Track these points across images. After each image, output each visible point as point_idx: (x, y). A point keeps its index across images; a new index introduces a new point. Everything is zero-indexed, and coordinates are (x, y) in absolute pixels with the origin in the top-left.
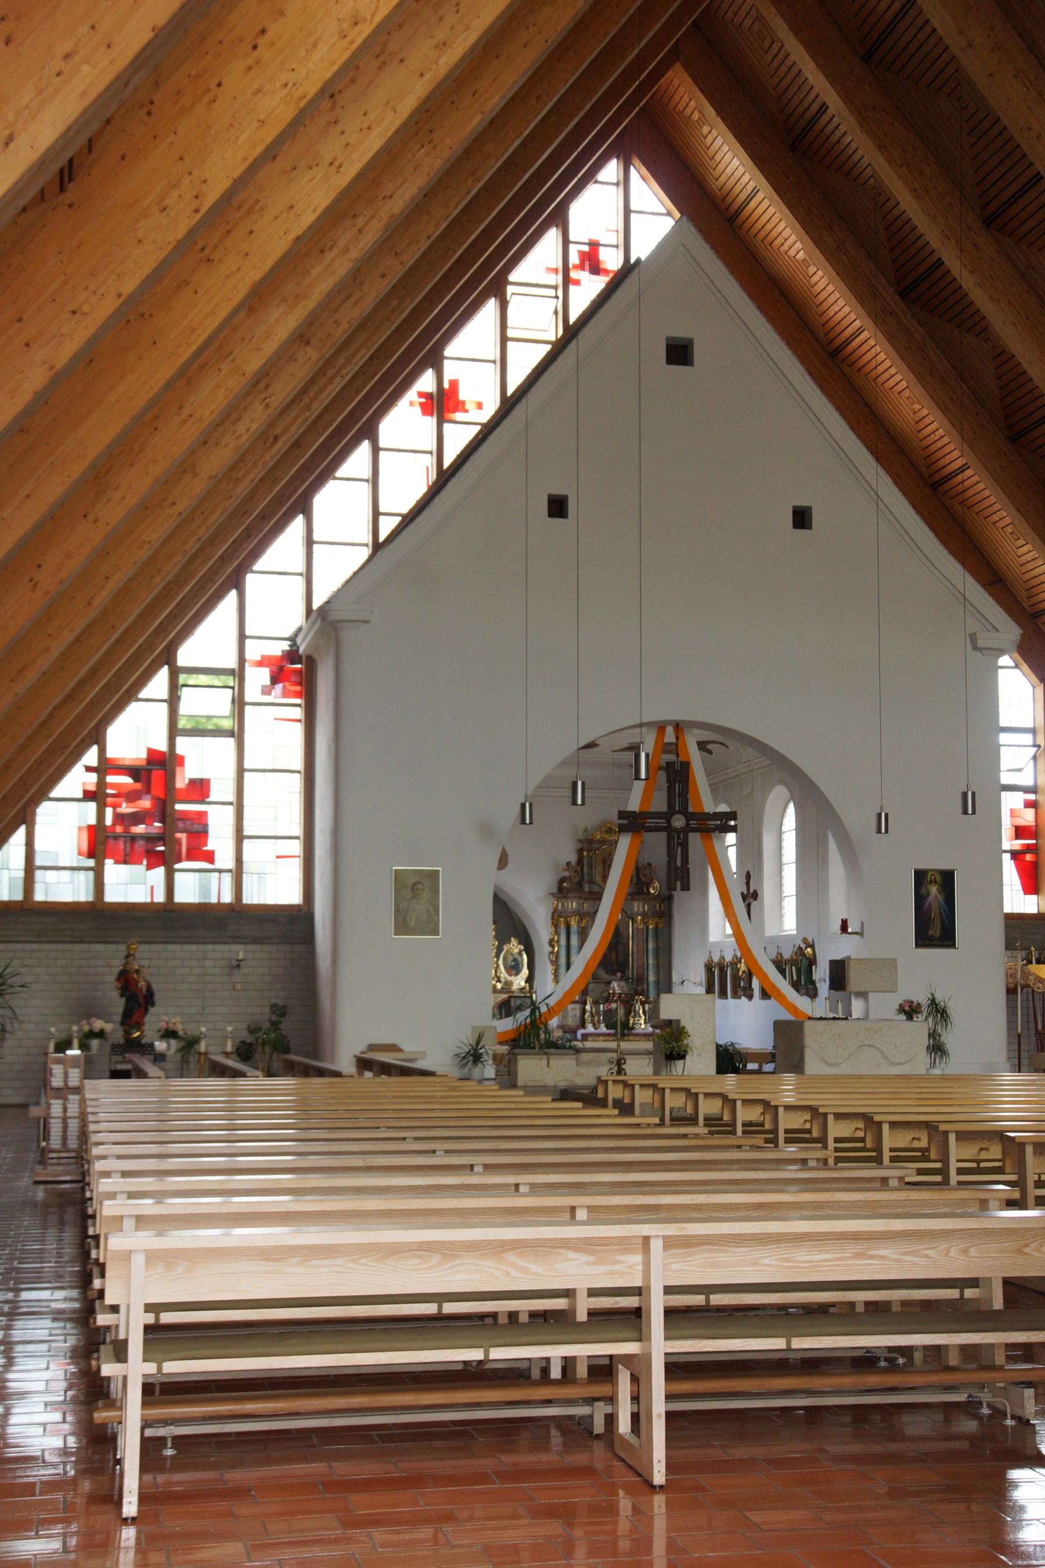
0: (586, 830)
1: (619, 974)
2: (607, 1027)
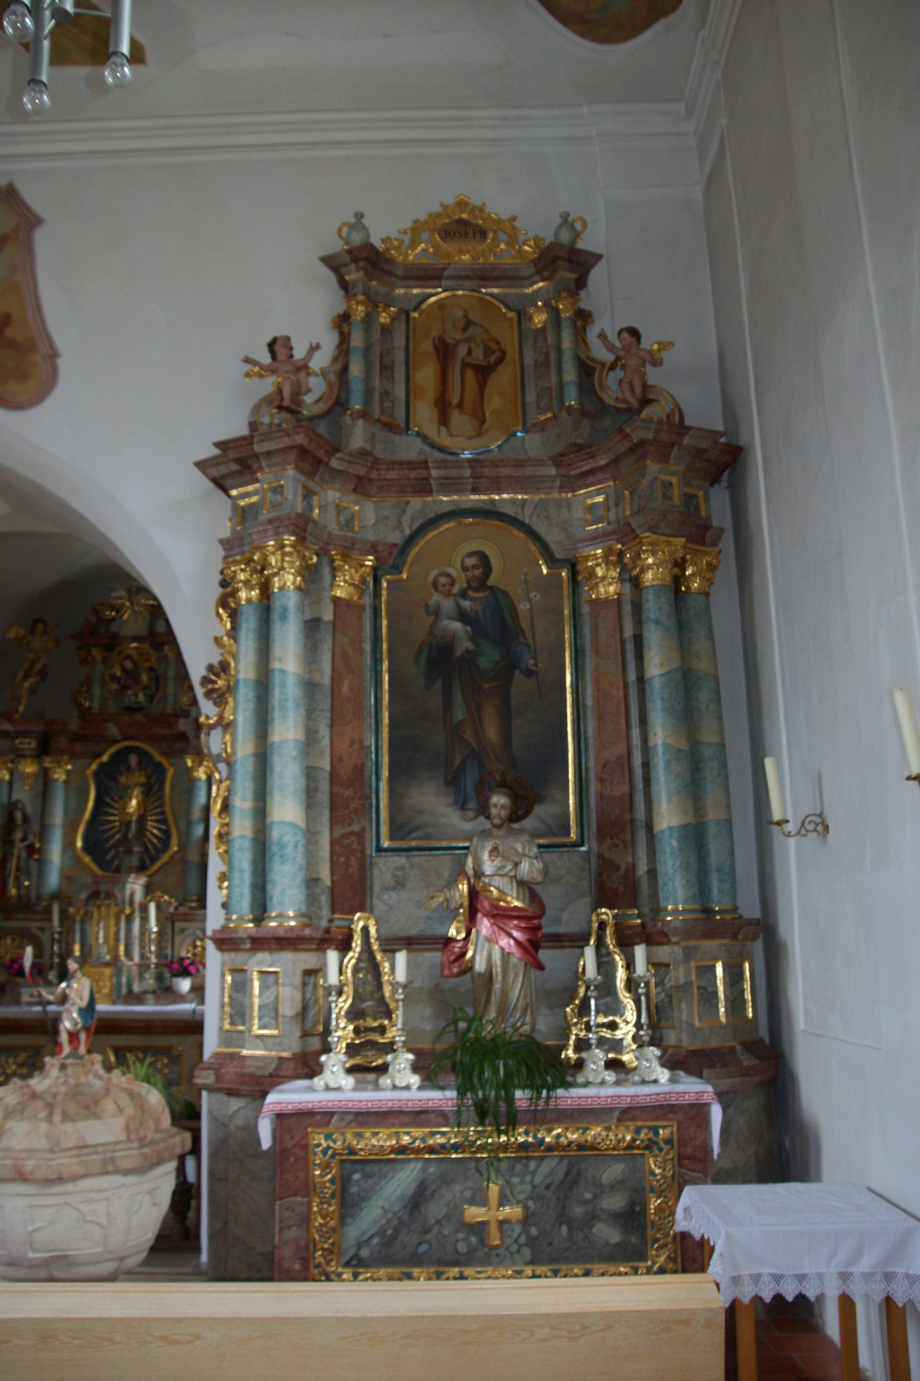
1: (499, 801)
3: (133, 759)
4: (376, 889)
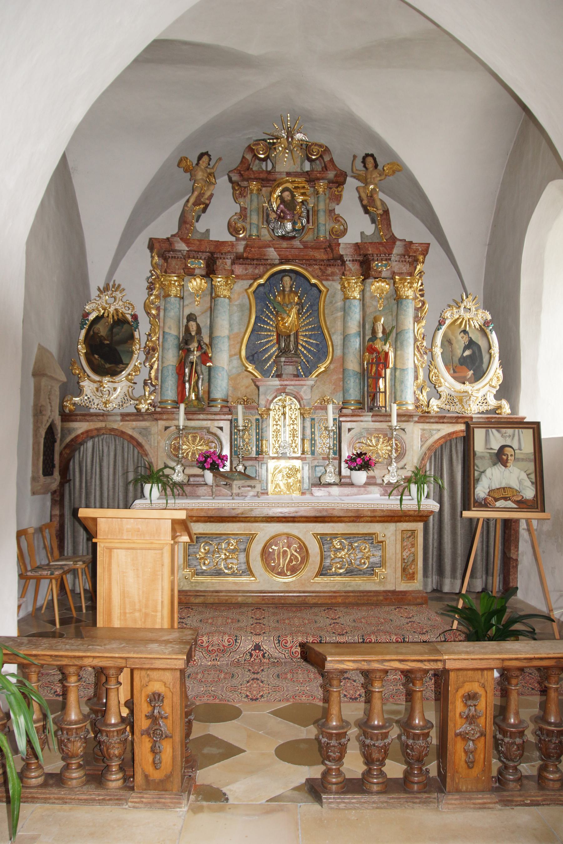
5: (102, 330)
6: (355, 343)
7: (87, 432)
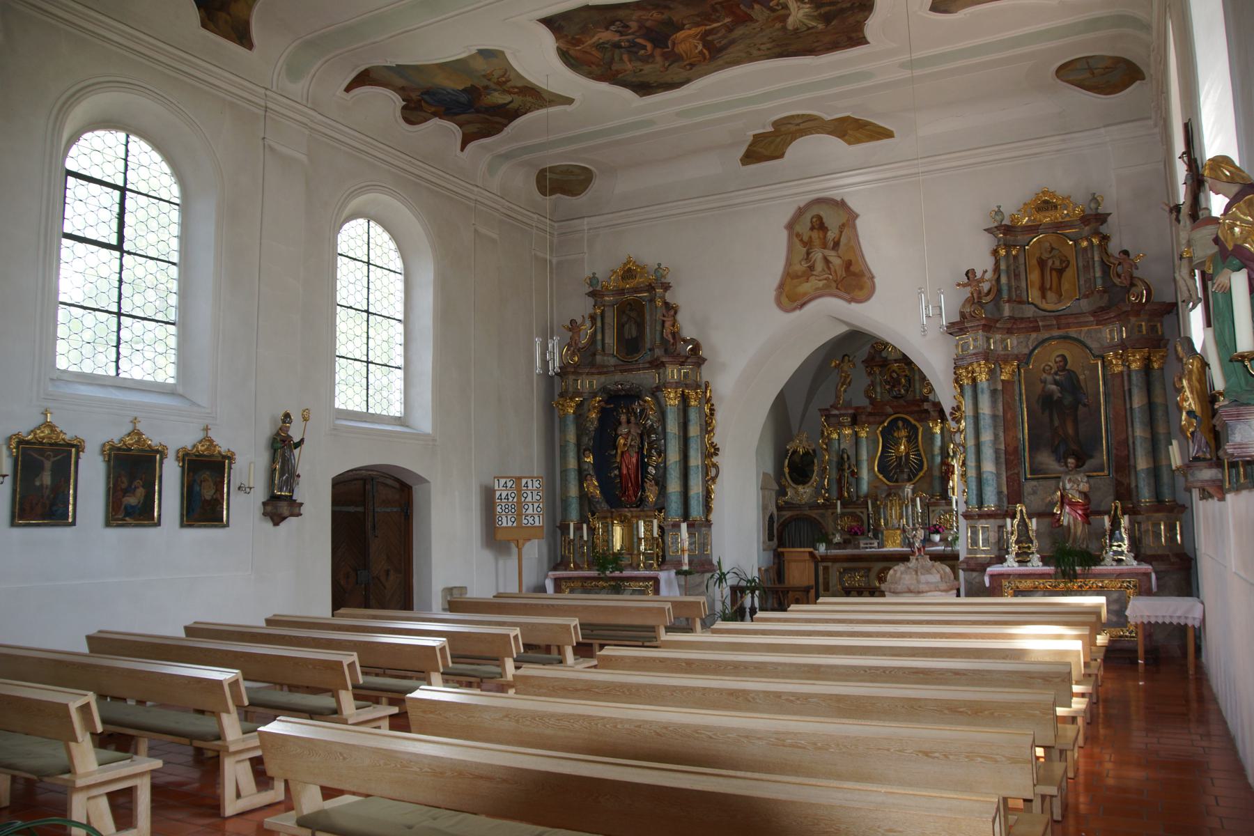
0: (999, 212)
1: (1071, 461)
2: (1045, 561)
3: (900, 424)
4: (1025, 494)
5: (796, 458)
6: (938, 459)
7: (791, 517)
